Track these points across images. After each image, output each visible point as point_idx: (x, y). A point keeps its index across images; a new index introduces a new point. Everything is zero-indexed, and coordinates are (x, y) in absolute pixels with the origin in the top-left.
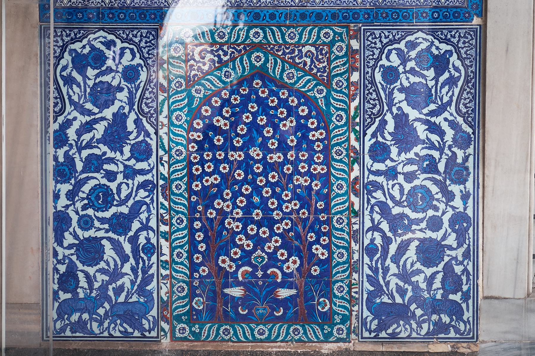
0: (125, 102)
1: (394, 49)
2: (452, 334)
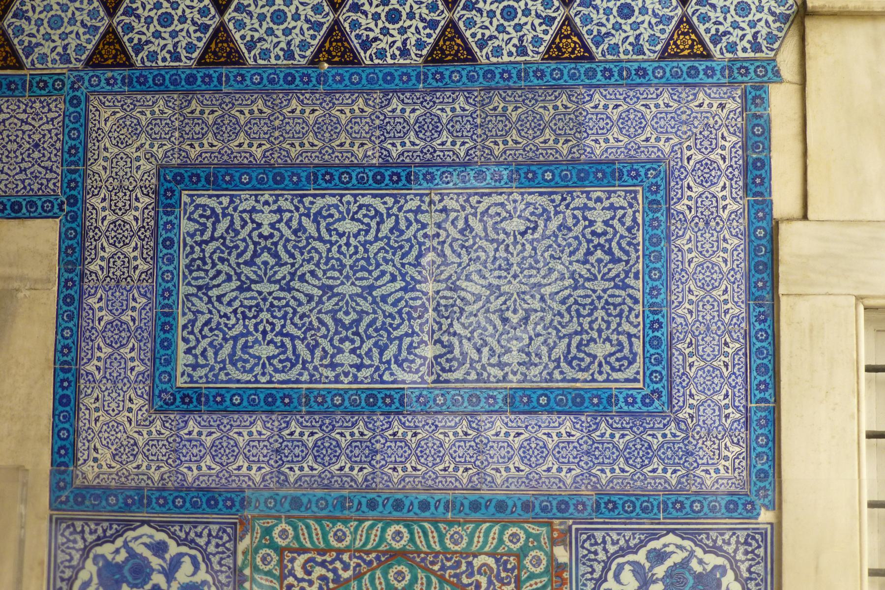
1: (628, 562)
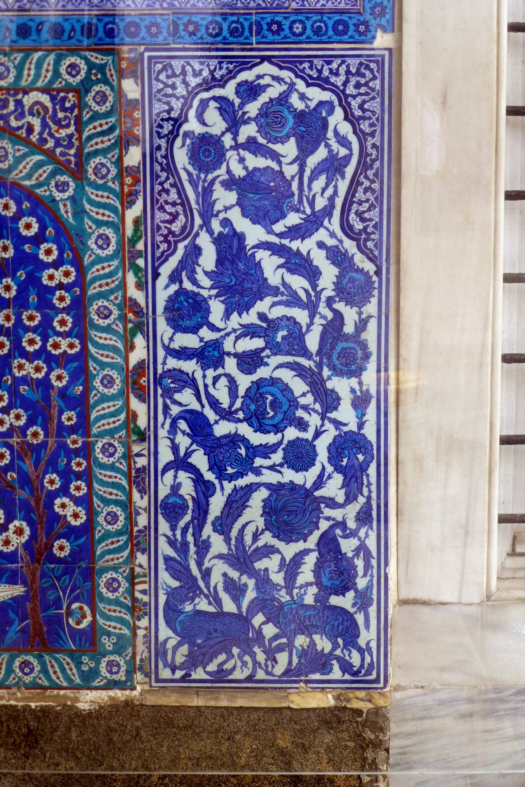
1: (214, 98)
2: (337, 673)
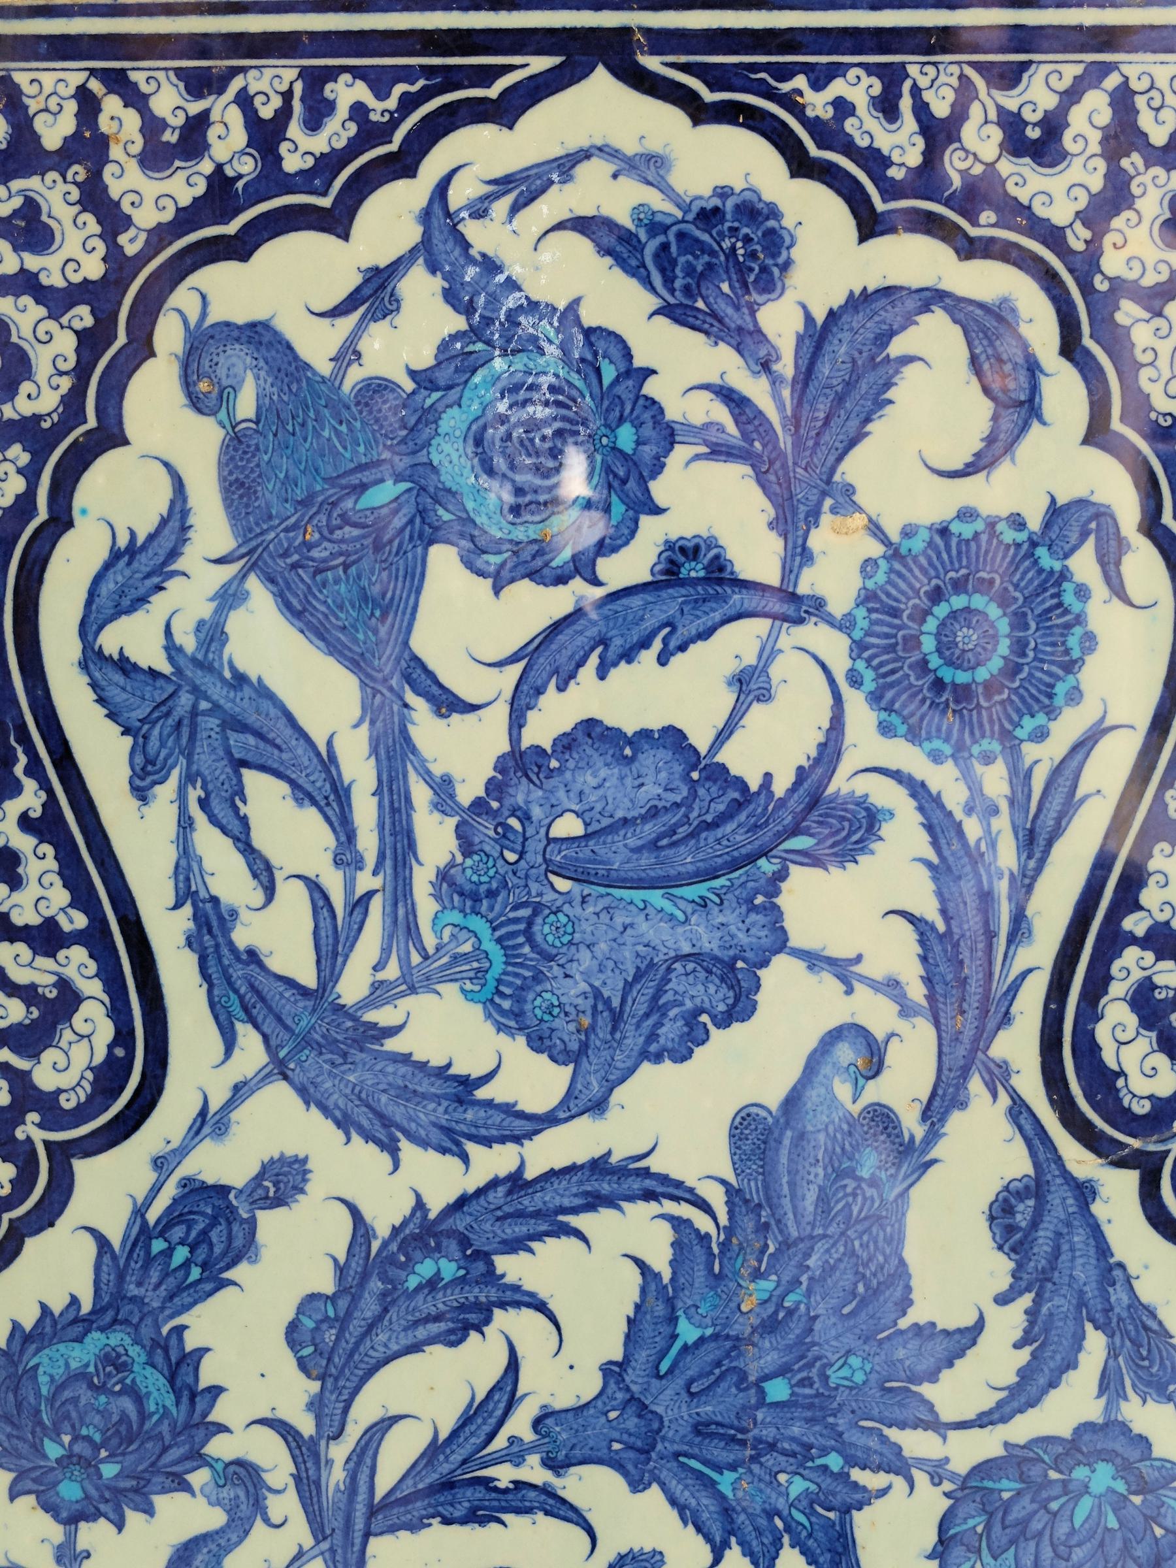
0: (891, 987)
